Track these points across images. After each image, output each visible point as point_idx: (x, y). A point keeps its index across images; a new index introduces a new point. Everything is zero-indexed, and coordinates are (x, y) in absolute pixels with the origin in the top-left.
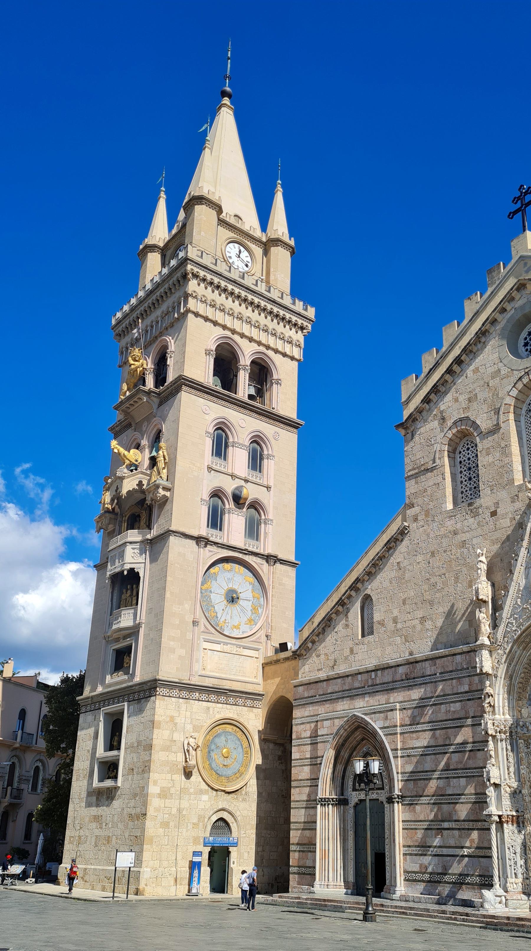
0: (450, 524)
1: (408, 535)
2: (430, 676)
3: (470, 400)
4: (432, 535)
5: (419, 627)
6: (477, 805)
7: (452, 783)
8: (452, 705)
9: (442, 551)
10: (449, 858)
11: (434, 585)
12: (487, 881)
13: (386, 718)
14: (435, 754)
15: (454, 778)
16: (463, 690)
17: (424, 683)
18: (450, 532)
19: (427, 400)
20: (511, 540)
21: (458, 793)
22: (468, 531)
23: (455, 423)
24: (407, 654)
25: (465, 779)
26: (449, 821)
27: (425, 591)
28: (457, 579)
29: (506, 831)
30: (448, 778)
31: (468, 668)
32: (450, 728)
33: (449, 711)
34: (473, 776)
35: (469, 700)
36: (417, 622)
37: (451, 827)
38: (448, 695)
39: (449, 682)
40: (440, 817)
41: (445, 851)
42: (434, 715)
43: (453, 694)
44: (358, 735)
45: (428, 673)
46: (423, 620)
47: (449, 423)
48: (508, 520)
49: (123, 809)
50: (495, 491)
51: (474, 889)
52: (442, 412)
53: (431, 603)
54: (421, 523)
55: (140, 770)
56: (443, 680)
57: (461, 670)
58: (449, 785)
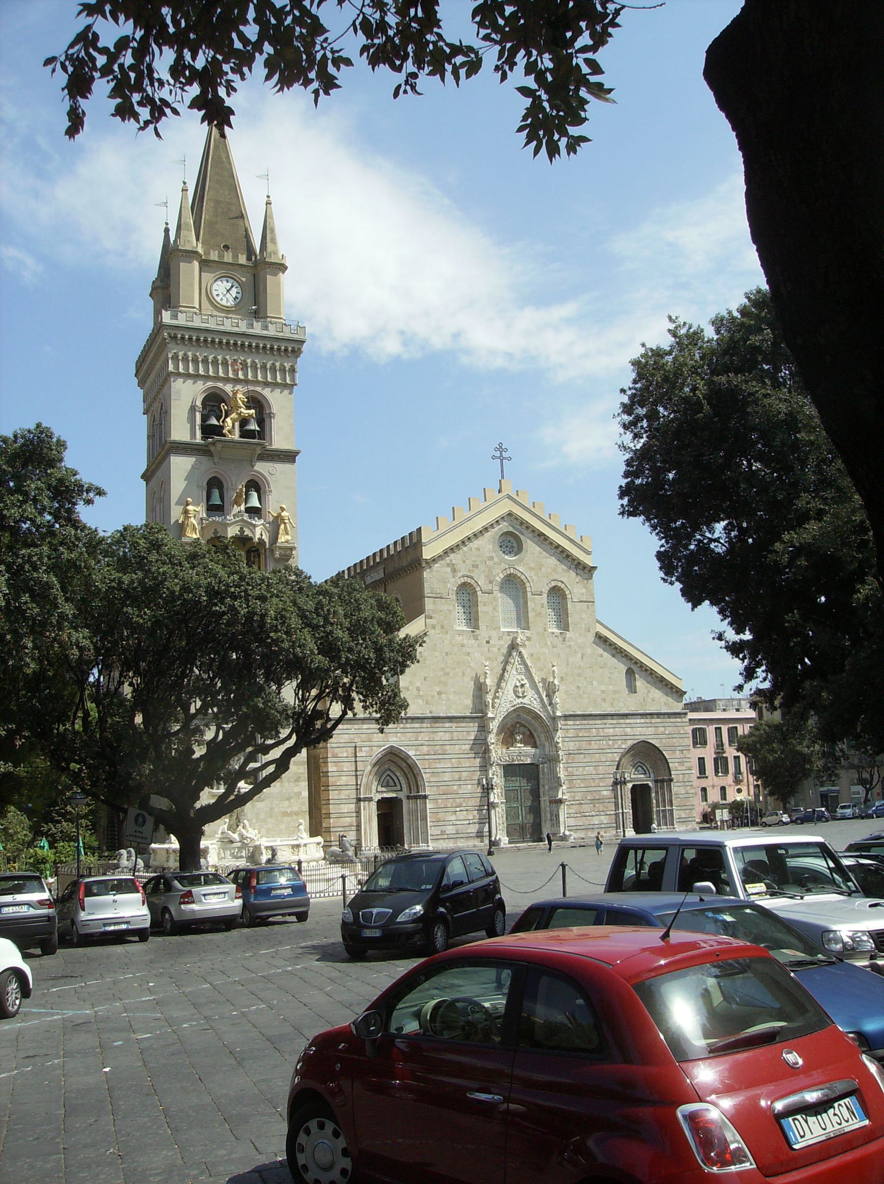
3: (473, 566)
5: (436, 696)
11: (448, 674)
13: (417, 750)
19: (446, 553)
23: (463, 576)
24: (428, 712)
28: (463, 674)
36: (436, 694)
40: (454, 805)
41: (458, 823)
44: (388, 757)
46: (439, 693)
47: (460, 574)
48: (496, 649)
49: (272, 809)
52: (453, 565)
53: (445, 684)
54: (439, 632)
55: (293, 780)
58: (460, 788)
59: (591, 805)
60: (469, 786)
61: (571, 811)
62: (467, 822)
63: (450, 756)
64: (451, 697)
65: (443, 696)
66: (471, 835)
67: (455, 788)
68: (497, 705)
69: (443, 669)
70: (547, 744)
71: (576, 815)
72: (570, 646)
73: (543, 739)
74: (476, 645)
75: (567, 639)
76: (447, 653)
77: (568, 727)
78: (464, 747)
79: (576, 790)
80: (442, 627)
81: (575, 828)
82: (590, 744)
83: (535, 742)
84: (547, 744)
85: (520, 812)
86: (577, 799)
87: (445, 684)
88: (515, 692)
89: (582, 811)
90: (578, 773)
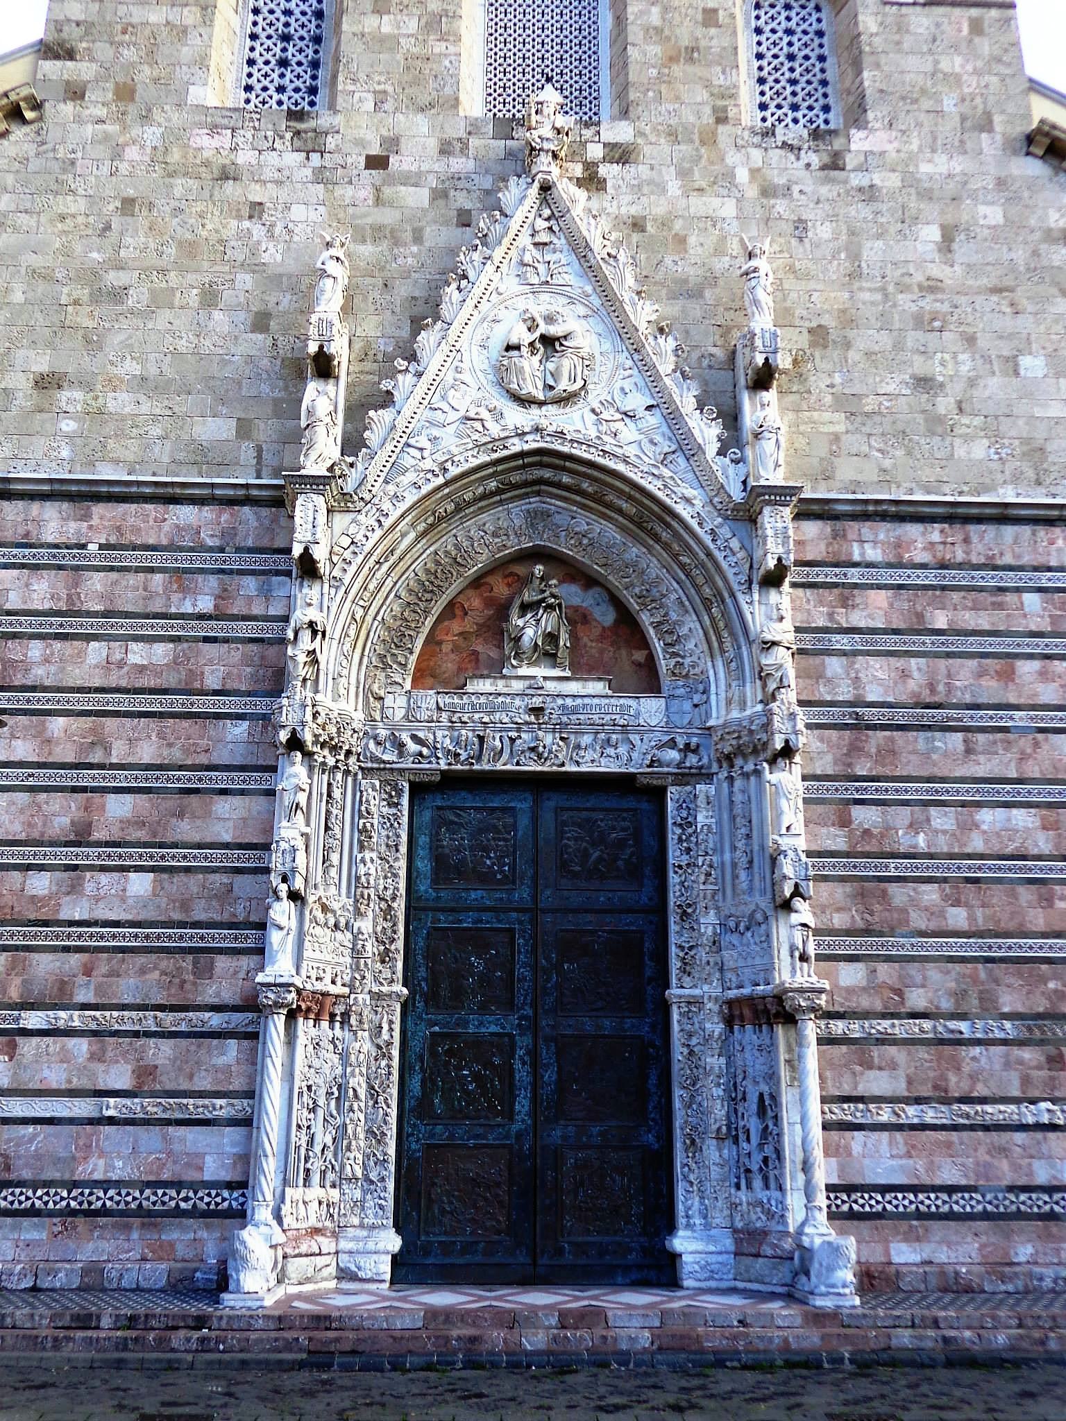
0: (207, 144)
1: (34, 127)
2: (56, 546)
4: (132, 153)
6: (190, 957)
7: (89, 887)
8: (133, 646)
9: (167, 208)
10: (31, 1129)
11: (118, 295)
12: (186, 1199)
14: (32, 789)
15: (103, 869)
16: (188, 608)
17: (23, 566)
18: (206, 164)
20: (427, 244)
21: (113, 916)
22: (279, 183)
25: (152, 875)
26: (55, 1007)
27: (76, 302)
28: (210, 298)
29: (302, 1040)
30: (75, 868)
31: (222, 550)
32: (117, 714)
33: (121, 664)
34: (187, 870)
35: (206, 640)
37: (61, 1024)
38: (127, 615)
39: (133, 579)
42: (53, 669)
43: (147, 616)
45: (50, 539)
46: (47, 383)
50: (386, 107)
51: (128, 1228)
54: (101, 112)
56: (112, 569)
57: (192, 549)
58: (74, 889)
59: (1027, 1054)
60: (140, 884)
61: (876, 1083)
62: (82, 1108)
63: (40, 701)
64: (120, 402)
65: (72, 398)
66: (99, 1199)
67: (40, 884)
68: (373, 437)
69: (92, 275)
70: (717, 674)
71: (912, 1113)
72: (869, 194)
73: (694, 644)
74: (308, 172)
75: (851, 161)
76: (128, 205)
77: (854, 576)
78: (138, 654)
79: (905, 945)
80: (125, 93)
81: (905, 1202)
82: (1007, 676)
83: (650, 666)
84: (717, 674)
85: (522, 1073)
86: (917, 999)
87: (92, 343)
88: (501, 376)
89: (956, 1084)
90: (921, 841)
